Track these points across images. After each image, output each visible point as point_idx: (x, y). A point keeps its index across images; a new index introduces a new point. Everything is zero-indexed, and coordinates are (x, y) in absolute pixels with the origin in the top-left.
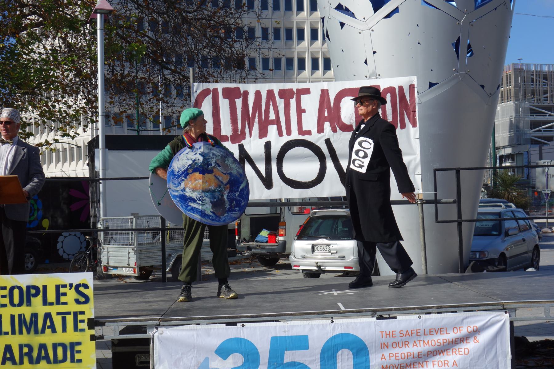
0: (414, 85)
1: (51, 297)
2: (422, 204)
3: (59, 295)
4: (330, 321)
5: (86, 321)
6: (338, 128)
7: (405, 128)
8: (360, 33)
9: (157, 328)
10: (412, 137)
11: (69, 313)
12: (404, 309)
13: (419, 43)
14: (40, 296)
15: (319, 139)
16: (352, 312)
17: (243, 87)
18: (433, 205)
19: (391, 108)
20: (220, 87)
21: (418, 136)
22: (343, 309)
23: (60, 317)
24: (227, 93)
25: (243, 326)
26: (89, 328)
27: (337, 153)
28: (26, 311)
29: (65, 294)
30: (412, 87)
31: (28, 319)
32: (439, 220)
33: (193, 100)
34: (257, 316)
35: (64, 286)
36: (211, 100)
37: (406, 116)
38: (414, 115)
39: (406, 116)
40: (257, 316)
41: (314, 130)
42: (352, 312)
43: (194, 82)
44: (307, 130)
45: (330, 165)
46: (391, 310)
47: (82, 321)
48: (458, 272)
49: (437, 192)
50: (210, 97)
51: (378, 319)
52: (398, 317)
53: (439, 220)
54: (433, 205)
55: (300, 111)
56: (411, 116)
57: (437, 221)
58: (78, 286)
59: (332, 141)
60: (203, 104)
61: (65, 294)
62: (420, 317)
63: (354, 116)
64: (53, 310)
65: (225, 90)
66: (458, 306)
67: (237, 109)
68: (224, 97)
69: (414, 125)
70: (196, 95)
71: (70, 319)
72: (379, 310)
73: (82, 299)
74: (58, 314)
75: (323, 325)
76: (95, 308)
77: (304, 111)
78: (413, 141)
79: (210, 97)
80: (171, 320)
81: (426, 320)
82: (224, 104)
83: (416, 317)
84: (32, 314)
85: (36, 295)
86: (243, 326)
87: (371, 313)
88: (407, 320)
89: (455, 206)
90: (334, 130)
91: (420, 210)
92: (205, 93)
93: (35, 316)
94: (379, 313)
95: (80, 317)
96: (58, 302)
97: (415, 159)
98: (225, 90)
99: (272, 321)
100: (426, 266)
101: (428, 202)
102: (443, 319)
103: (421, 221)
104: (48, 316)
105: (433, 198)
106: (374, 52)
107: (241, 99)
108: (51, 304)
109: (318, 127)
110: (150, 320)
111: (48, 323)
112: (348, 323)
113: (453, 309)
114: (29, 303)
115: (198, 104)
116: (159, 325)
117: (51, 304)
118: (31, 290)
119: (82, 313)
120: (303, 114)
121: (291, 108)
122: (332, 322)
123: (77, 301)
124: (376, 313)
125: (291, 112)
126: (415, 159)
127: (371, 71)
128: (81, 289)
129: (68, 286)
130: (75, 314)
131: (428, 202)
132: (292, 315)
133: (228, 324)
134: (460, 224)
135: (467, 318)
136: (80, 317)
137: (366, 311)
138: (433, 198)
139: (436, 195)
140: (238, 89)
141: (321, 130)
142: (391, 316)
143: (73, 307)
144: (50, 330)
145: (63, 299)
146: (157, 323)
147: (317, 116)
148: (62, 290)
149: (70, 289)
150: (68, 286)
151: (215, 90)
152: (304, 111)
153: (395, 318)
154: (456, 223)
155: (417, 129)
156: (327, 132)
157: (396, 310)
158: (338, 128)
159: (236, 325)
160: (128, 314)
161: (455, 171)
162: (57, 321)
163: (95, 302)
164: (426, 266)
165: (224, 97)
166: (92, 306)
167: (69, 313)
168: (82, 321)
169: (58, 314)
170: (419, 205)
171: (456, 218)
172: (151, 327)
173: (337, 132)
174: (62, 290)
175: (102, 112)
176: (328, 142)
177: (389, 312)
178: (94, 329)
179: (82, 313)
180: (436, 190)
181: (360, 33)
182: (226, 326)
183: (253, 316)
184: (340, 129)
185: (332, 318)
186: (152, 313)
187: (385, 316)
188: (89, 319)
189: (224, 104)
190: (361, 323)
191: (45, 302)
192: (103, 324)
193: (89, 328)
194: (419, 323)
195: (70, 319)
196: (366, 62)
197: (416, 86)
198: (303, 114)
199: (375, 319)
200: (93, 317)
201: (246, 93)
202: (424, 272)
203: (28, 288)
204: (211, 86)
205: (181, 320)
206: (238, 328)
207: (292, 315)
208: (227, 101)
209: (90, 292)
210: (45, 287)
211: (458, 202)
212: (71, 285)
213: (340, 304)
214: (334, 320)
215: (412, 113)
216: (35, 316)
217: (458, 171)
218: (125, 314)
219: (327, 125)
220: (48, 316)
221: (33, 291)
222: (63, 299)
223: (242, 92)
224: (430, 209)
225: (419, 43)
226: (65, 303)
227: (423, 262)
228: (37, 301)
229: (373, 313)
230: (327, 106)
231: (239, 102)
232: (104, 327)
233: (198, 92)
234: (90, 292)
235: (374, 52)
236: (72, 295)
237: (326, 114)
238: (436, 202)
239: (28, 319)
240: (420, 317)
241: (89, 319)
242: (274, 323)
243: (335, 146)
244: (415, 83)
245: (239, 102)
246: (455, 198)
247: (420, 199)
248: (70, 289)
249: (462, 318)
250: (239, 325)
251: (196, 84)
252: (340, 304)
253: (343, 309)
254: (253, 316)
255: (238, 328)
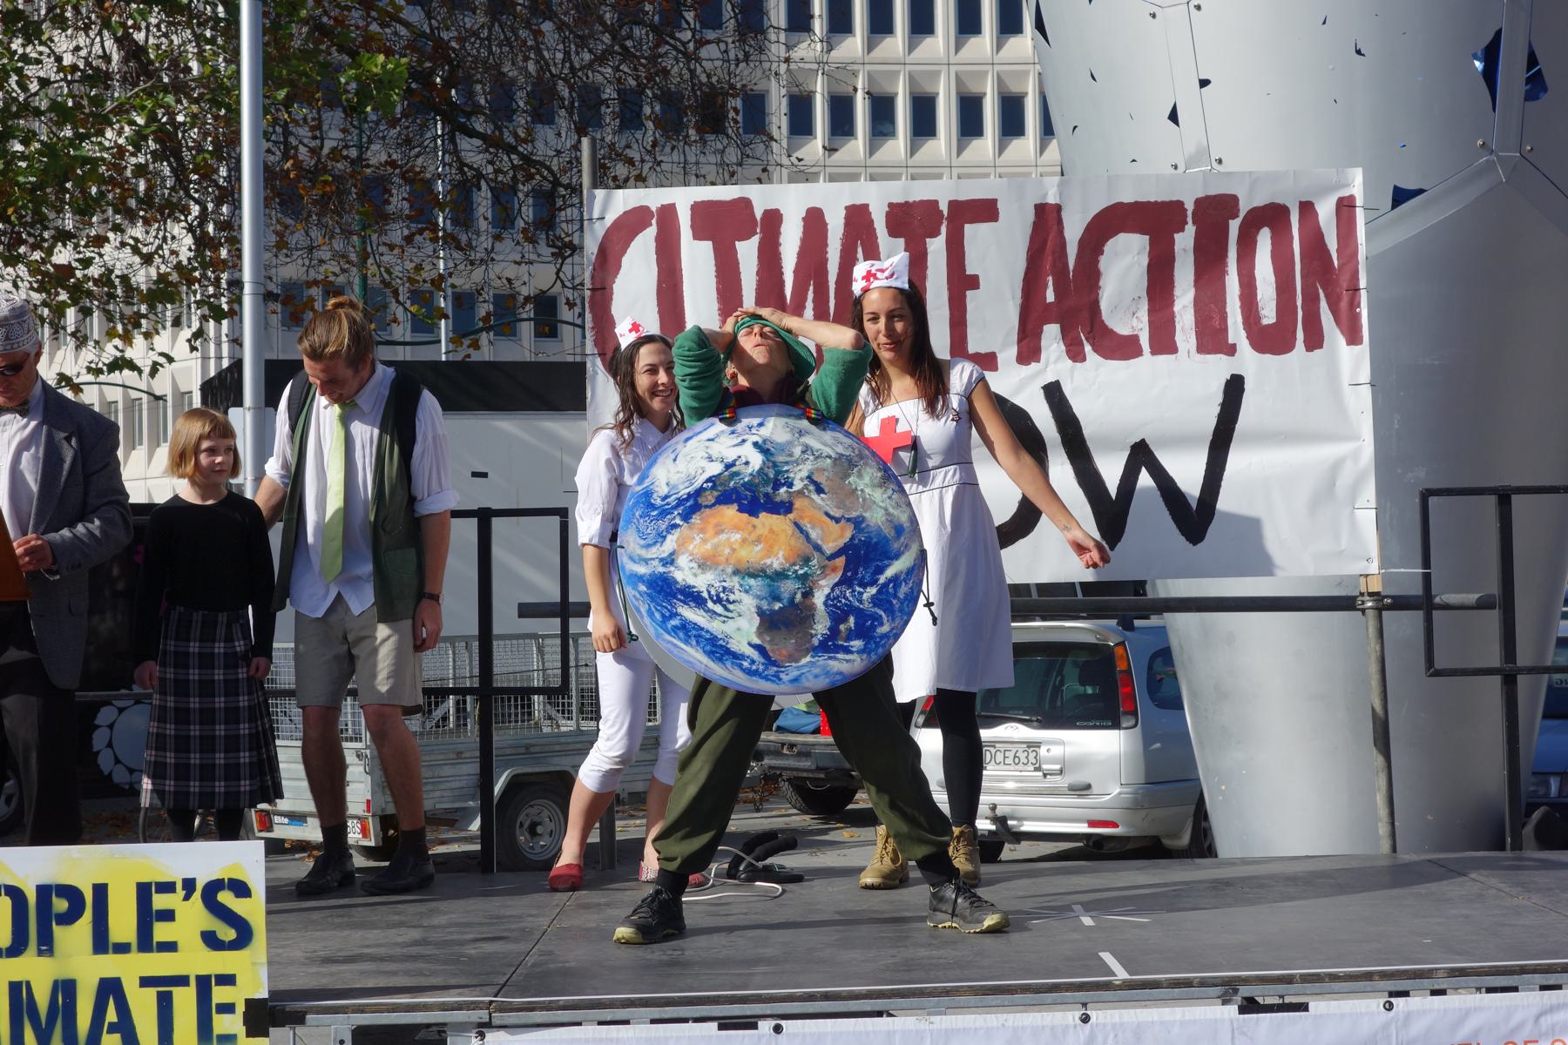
0: (1352, 198)
1: (123, 925)
2: (1379, 610)
3: (147, 917)
4: (1078, 1014)
5: (241, 1008)
6: (1088, 348)
7: (1320, 346)
8: (1154, 16)
9: (482, 1035)
10: (1346, 379)
11: (182, 981)
12: (1334, 978)
13: (1359, 52)
14: (85, 922)
15: (1021, 386)
16: (1155, 985)
17: (761, 197)
18: (1418, 616)
19: (1272, 278)
20: (683, 198)
21: (1365, 375)
22: (1121, 974)
23: (152, 992)
24: (710, 221)
25: (778, 1029)
26: (250, 1033)
27: (1086, 432)
28: (37, 972)
29: (168, 916)
30: (1345, 207)
31: (42, 999)
32: (1438, 665)
33: (591, 247)
34: (827, 997)
35: (167, 888)
36: (653, 245)
37: (1324, 305)
38: (1354, 303)
39: (1324, 305)
40: (827, 997)
41: (1008, 355)
42: (1155, 985)
43: (595, 186)
44: (983, 351)
45: (1061, 471)
46: (1289, 980)
47: (228, 1008)
48: (1503, 848)
49: (1434, 571)
50: (651, 233)
51: (1243, 1010)
52: (1312, 1006)
53: (1438, 665)
54: (1418, 616)
55: (962, 283)
56: (1344, 304)
57: (1433, 671)
58: (213, 887)
59: (1067, 390)
60: (625, 260)
61: (168, 916)
62: (1389, 1007)
63: (1146, 307)
64: (130, 968)
65: (698, 209)
66: (1523, 970)
67: (743, 277)
68: (698, 235)
69: (1353, 338)
70: (600, 230)
71: (185, 1000)
72: (1246, 981)
73: (228, 934)
74: (146, 982)
75: (1053, 1028)
76: (270, 963)
77: (974, 282)
78: (1347, 390)
79: (651, 233)
80: (531, 1008)
81: (1408, 1016)
82: (697, 258)
83: (1375, 1004)
84: (56, 983)
85: (69, 918)
86: (778, 1029)
87: (1218, 990)
88: (1342, 1016)
89: (1493, 617)
90: (1076, 355)
91: (1372, 631)
92: (634, 221)
93: (66, 989)
94: (1245, 991)
95: (220, 994)
96: (145, 943)
97: (1355, 455)
98: (698, 209)
99: (879, 1014)
100: (1393, 824)
101: (1400, 603)
102: (1467, 1013)
103: (1374, 668)
104: (110, 989)
105: (1416, 590)
106: (1204, 83)
107: (756, 240)
108: (122, 948)
109: (1020, 341)
110: (459, 1007)
111: (111, 1016)
112: (1139, 1025)
113: (1501, 980)
114: (46, 945)
115: (608, 261)
116: (488, 1025)
117: (122, 948)
118: (54, 899)
119: (227, 980)
120: (969, 293)
121: (929, 272)
122: (1085, 1019)
123: (211, 940)
124: (1236, 991)
125: (929, 284)
126: (1355, 455)
127: (1190, 148)
128: (225, 897)
129: (179, 886)
130: (204, 984)
131: (1400, 603)
132: (947, 992)
133: (726, 1024)
134: (1510, 680)
135: (1552, 1010)
136: (220, 994)
137: (1203, 983)
138: (1416, 590)
139: (1427, 578)
140: (745, 204)
141: (1029, 351)
142: (1288, 1000)
143: (196, 960)
144: (117, 1037)
145: (161, 932)
146: (482, 1015)
147: (1019, 301)
148: (160, 901)
149: (187, 898)
150: (179, 886)
151: (668, 212)
152: (974, 282)
153: (1303, 1007)
154: (1498, 679)
155: (1364, 349)
156: (1052, 359)
157: (1306, 979)
158: (1088, 348)
159: (754, 1026)
160: (382, 982)
161: (1492, 500)
162: (143, 1005)
163: (268, 939)
164: (1393, 824)
165: (698, 235)
166: (263, 958)
167: (182, 981)
168: (228, 1008)
169: (146, 982)
170: (1370, 613)
171: (1494, 658)
172: (462, 1028)
173: (1084, 359)
174: (160, 901)
175: (255, 283)
176: (1053, 392)
177: (1281, 988)
178: (266, 1035)
179: (227, 980)
180: (1426, 563)
181: (1154, 16)
182: (722, 1027)
183: (811, 998)
184: (1096, 350)
185: (1085, 1005)
186: (463, 981)
187: (1269, 1001)
188: (249, 1002)
189: (697, 258)
190: (1183, 1023)
191: (101, 943)
192: (298, 1019)
193: (249, 1034)
194: (1386, 1026)
195: (185, 1000)
196: (1173, 117)
197: (1359, 202)
198: (969, 293)
199: (1232, 1009)
200: (266, 996)
201: (773, 219)
202: (1385, 846)
203: (44, 891)
204: (653, 197)
205: (566, 1007)
206: (760, 1038)
207: (947, 992)
208: (707, 247)
209: (253, 909)
210: (101, 891)
211: (1505, 602)
212: (189, 885)
213: (1107, 957)
214: (1093, 1014)
215: (1345, 297)
216: (66, 989)
217: (1504, 497)
218: (370, 983)
219: (1051, 332)
220: (110, 989)
221: (60, 905)
222: (161, 932)
223: (758, 214)
224: (1406, 625)
225: (1359, 52)
226: (170, 947)
227: (1383, 812)
228: (75, 937)
229: (1227, 990)
230: (1054, 264)
231: (748, 252)
232: (300, 1030)
233: (610, 218)
234: (253, 909)
235: (1204, 83)
236: (191, 918)
237: (1050, 296)
238: (1424, 603)
239: (42, 999)
240: (1389, 1007)
241: (249, 1002)
242: (885, 1020)
243: (1079, 407)
244: (1356, 185)
245: (748, 252)
246: (1493, 588)
247: (1370, 594)
248: (187, 898)
249: (1535, 1011)
250: (766, 1026)
251: (600, 194)
252: (1107, 957)
253: (1121, 974)
254: (811, 998)
255: (760, 1038)
